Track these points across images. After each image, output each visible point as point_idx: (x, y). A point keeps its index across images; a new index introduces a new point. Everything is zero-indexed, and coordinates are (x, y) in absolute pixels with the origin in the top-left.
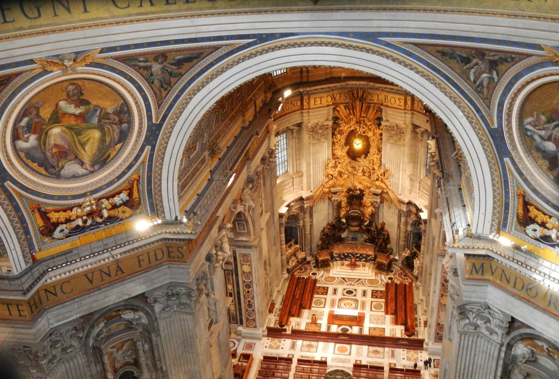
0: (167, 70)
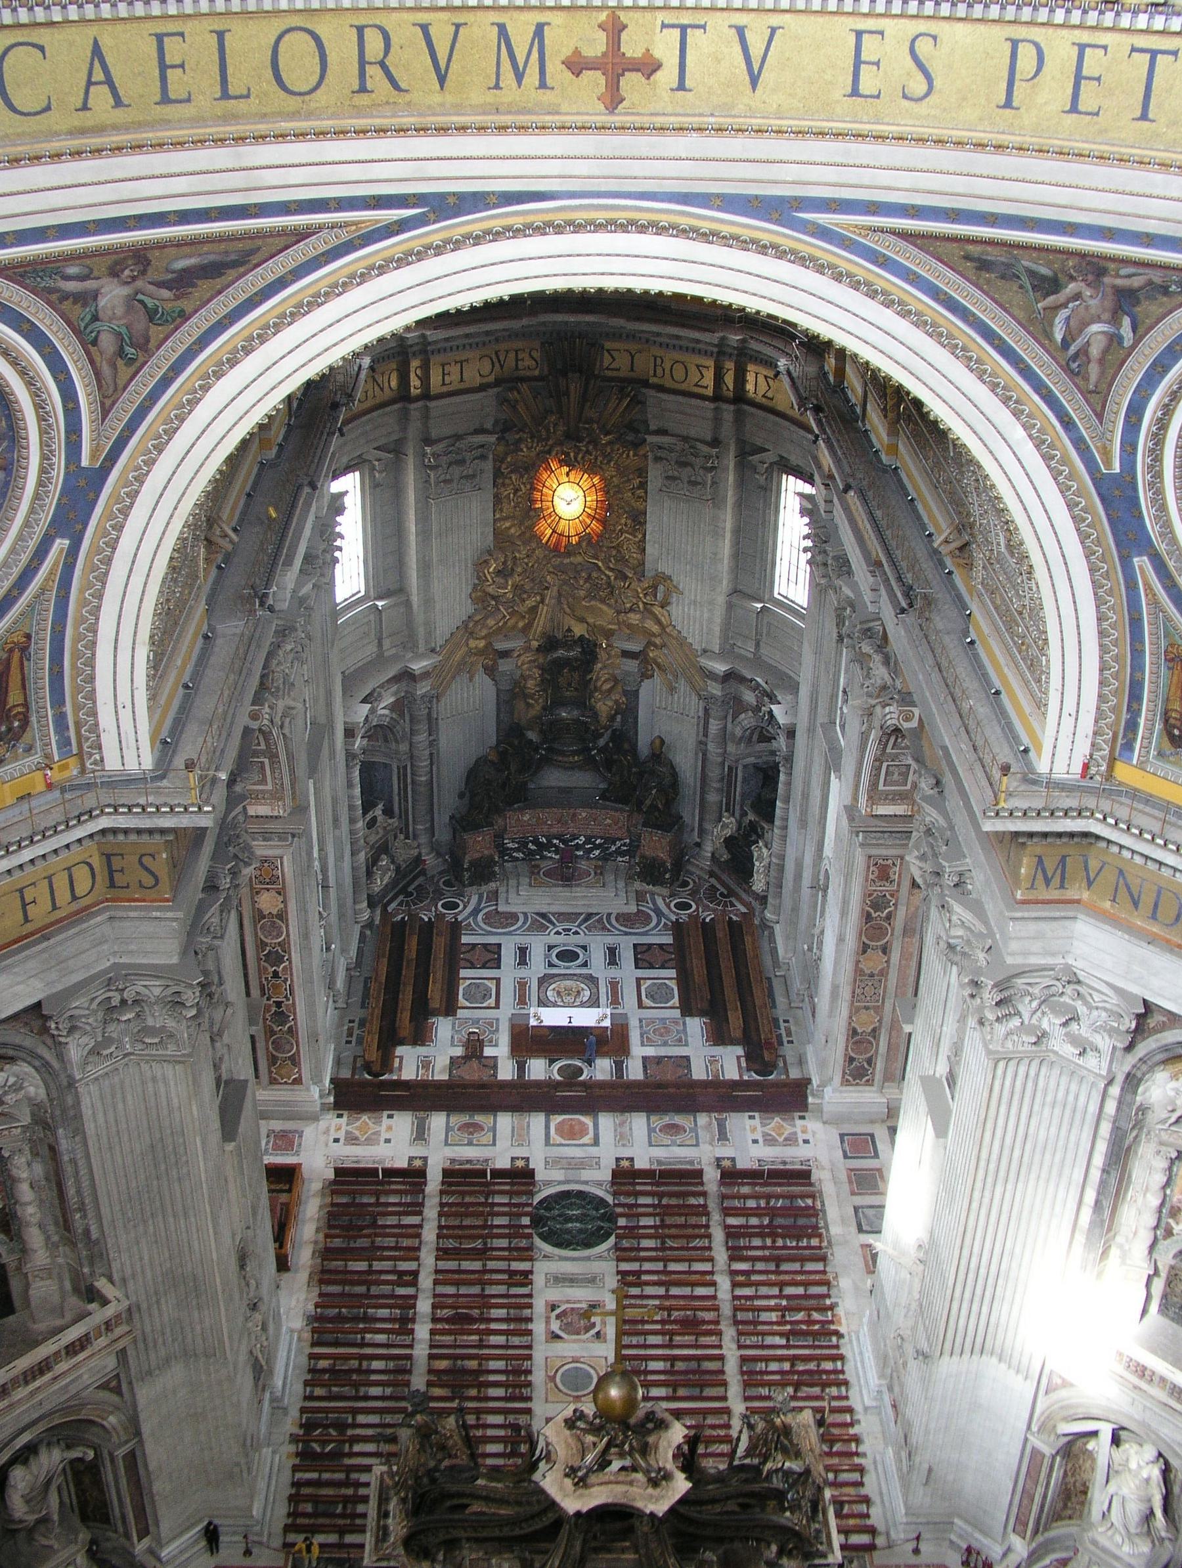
0: (141, 302)
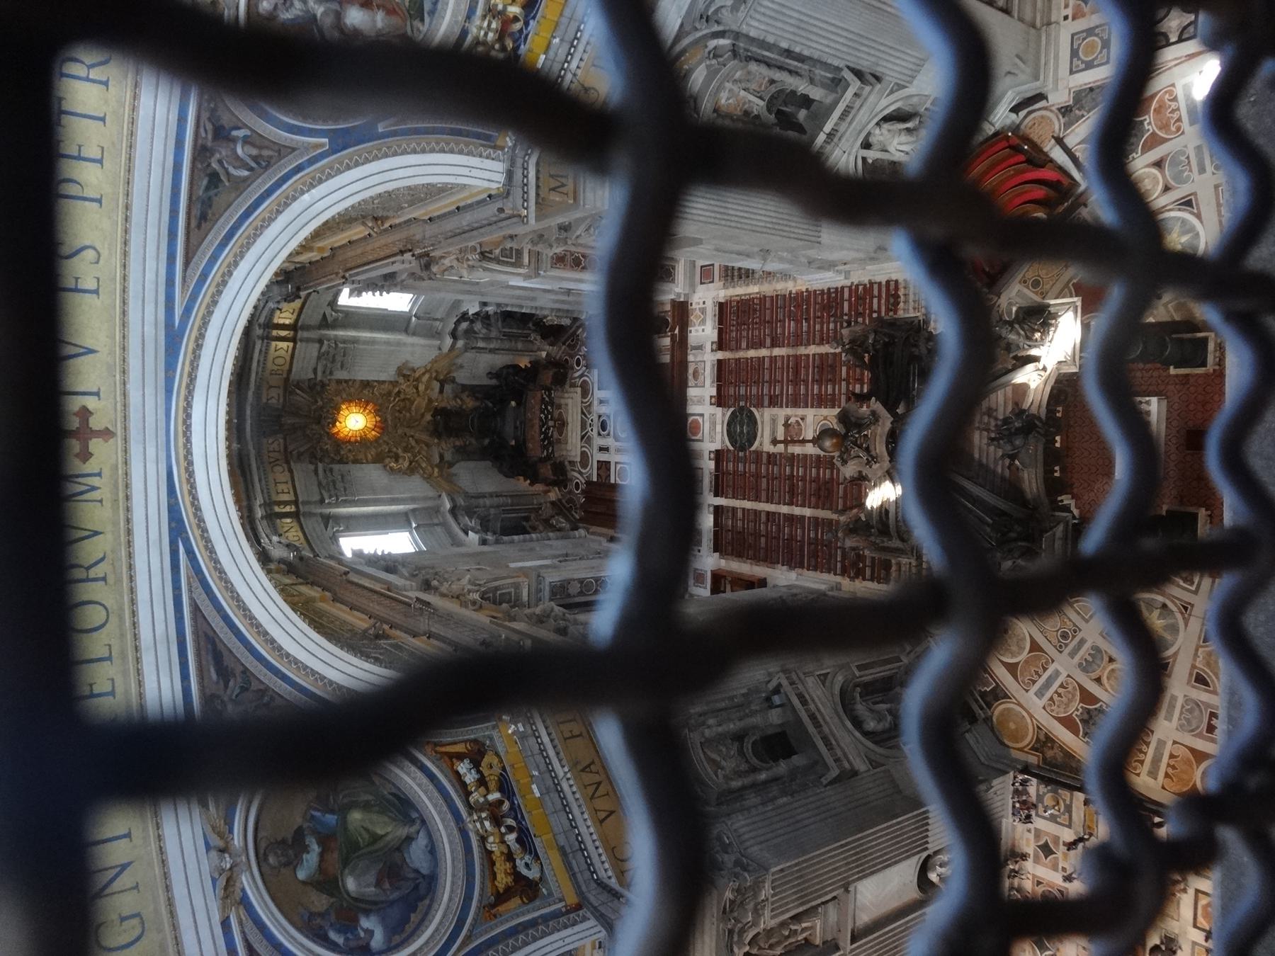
0: (237, 696)
